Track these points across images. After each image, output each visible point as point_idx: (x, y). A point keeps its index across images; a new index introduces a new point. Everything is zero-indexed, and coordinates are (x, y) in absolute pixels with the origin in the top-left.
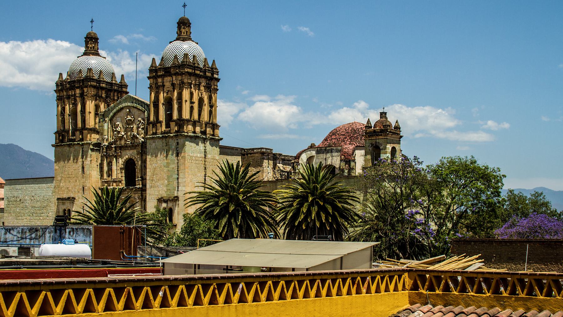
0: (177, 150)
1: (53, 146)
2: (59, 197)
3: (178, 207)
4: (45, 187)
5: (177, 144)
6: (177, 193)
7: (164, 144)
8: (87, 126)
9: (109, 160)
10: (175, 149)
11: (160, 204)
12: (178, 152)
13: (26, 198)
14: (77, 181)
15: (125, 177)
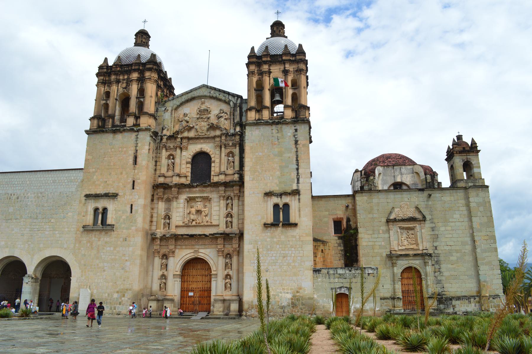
0: (296, 138)
1: (87, 132)
2: (88, 193)
3: (299, 202)
4: (65, 181)
5: (294, 131)
6: (298, 186)
7: (275, 131)
8: (145, 110)
9: (168, 153)
10: (292, 136)
11: (269, 199)
12: (296, 139)
13: (29, 194)
14: (124, 173)
15: (191, 173)
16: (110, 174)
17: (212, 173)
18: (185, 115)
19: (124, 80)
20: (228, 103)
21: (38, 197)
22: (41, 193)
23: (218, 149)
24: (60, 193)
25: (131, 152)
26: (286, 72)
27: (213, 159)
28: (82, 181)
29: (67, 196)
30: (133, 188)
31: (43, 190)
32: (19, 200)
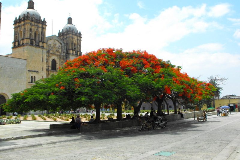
2: (29, 70)
13: (7, 67)
14: (40, 64)
16: (35, 64)
17: (57, 68)
18: (50, 44)
19: (37, 26)
20: (61, 44)
21: (10, 68)
22: (11, 67)
23: (59, 60)
24: (19, 68)
25: (42, 57)
26: (77, 39)
27: (57, 63)
28: (27, 65)
29: (22, 70)
30: (43, 70)
31: (12, 66)
32: (2, 69)
